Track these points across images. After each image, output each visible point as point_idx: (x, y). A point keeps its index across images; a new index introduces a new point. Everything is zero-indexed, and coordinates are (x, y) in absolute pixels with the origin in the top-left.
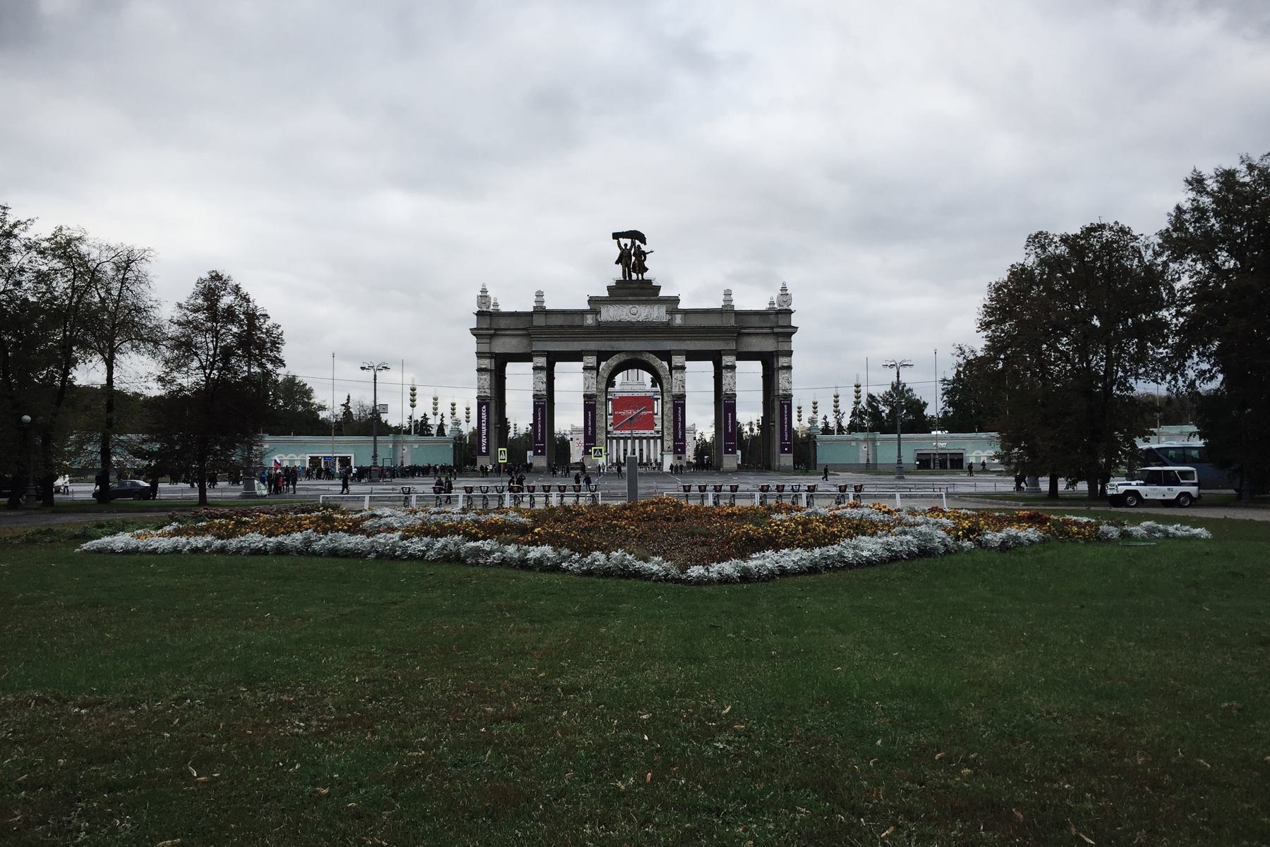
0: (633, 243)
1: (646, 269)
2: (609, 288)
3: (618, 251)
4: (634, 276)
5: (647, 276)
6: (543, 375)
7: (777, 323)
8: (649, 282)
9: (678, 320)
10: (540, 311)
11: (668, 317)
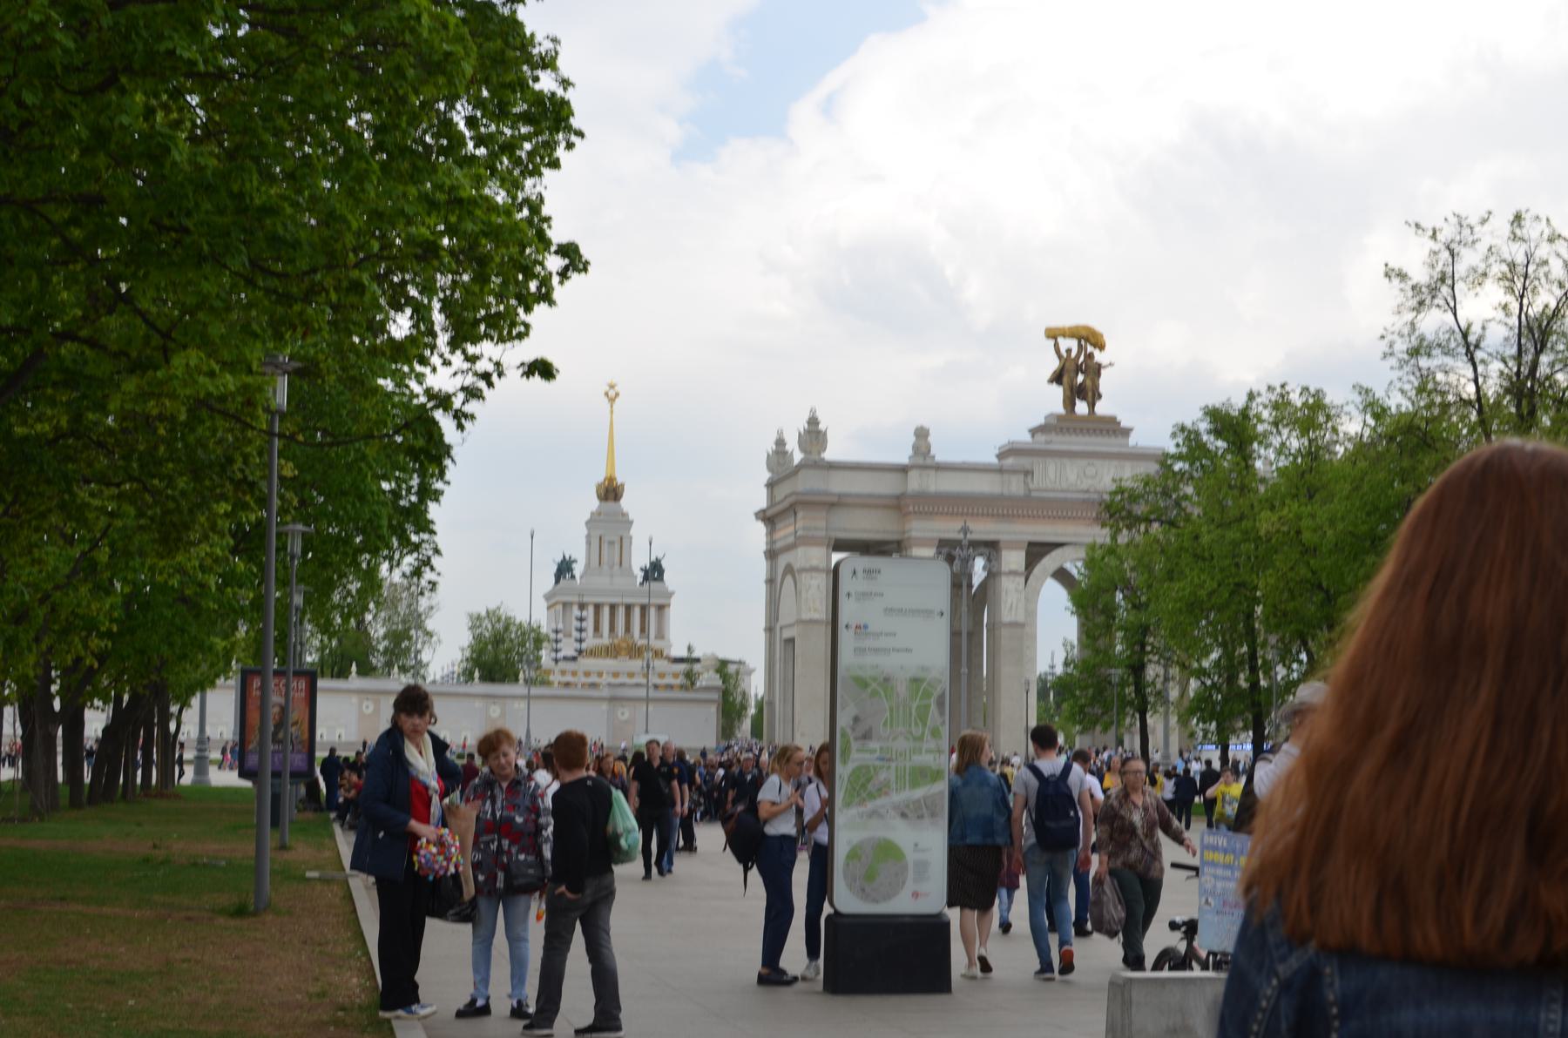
5: (1102, 408)
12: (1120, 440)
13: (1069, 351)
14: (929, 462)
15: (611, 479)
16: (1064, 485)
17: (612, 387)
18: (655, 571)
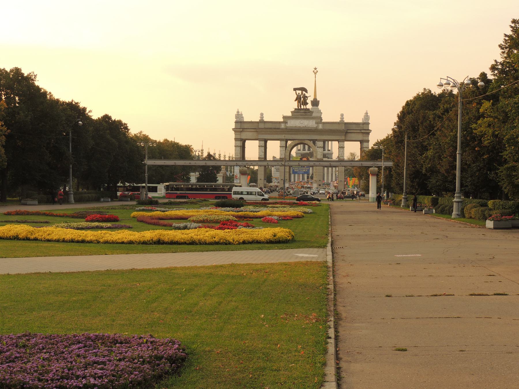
0: (302, 93)
2: (292, 112)
3: (296, 96)
4: (302, 107)
6: (263, 149)
9: (320, 127)
10: (262, 121)
11: (316, 125)
17: (316, 69)
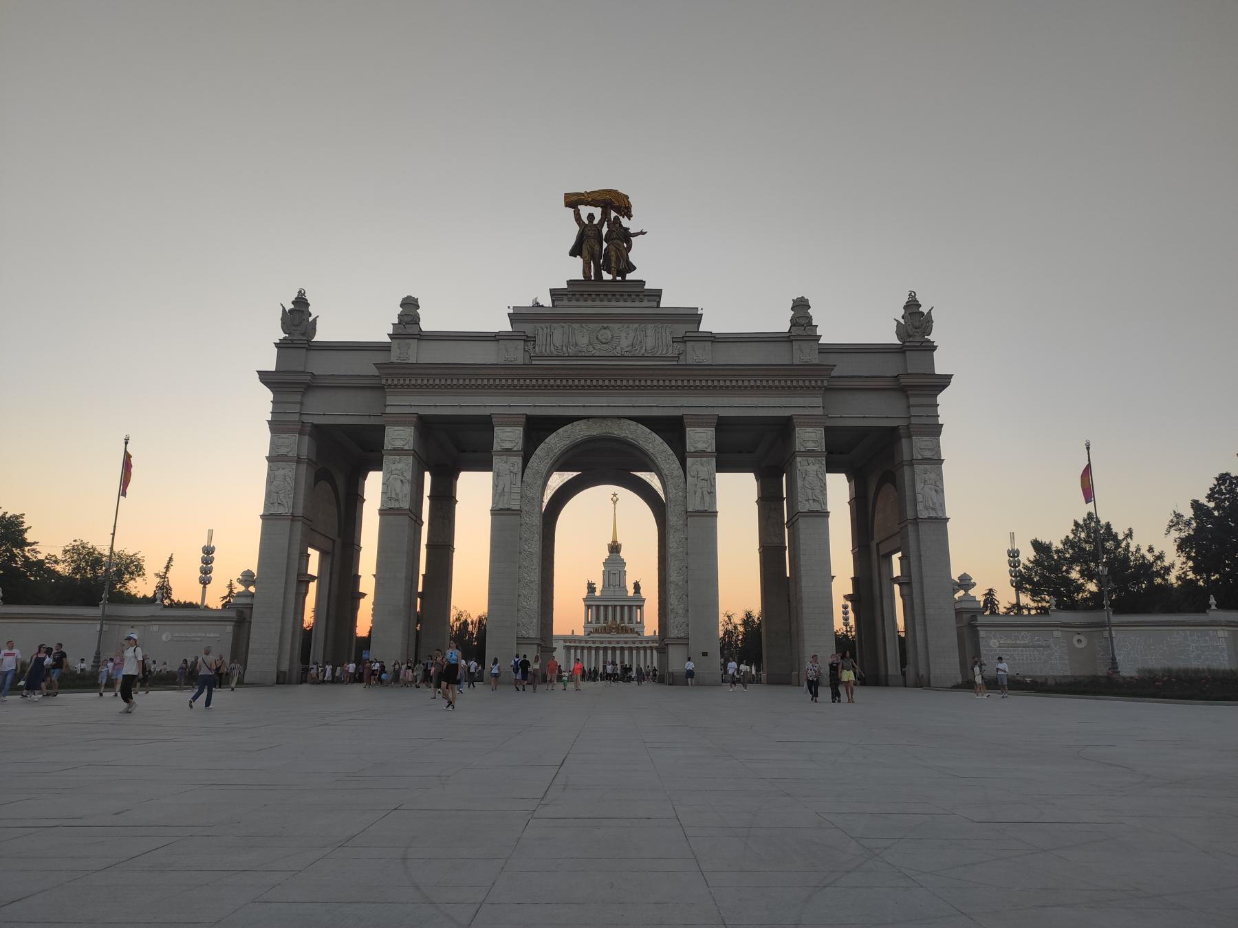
0: (605, 215)
1: (632, 268)
2: (555, 294)
3: (576, 229)
5: (629, 277)
7: (909, 369)
8: (642, 283)
9: (698, 355)
12: (646, 303)
13: (591, 217)
14: (411, 330)
15: (615, 542)
16: (572, 351)
18: (637, 587)
